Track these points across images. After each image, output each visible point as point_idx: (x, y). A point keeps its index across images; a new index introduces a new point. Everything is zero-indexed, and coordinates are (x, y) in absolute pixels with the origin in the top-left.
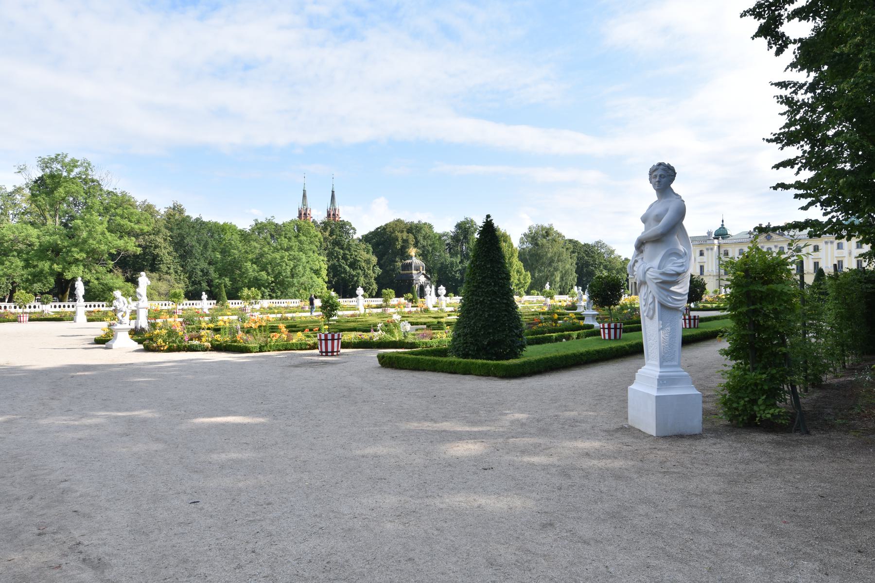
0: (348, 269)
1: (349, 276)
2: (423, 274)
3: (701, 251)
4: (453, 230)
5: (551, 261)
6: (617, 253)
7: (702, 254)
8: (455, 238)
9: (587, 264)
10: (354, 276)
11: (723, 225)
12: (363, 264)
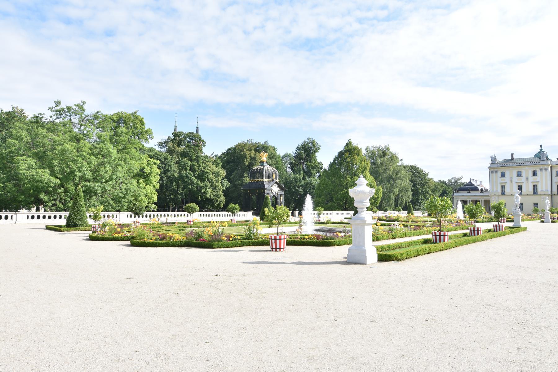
0: (195, 180)
1: (197, 187)
2: (276, 183)
3: (534, 172)
4: (295, 151)
5: (390, 178)
6: (430, 176)
8: (298, 157)
10: (201, 187)
11: (541, 150)
12: (211, 176)
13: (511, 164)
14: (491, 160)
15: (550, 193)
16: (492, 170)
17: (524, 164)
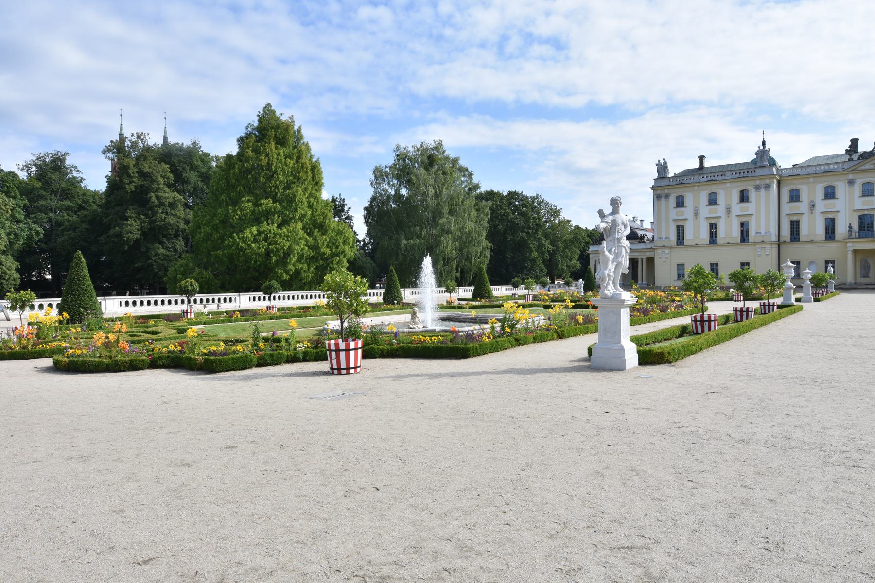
7: (744, 197)
9: (513, 228)
13: (696, 177)
14: (658, 171)
15: (774, 238)
16: (659, 192)
17: (723, 177)
